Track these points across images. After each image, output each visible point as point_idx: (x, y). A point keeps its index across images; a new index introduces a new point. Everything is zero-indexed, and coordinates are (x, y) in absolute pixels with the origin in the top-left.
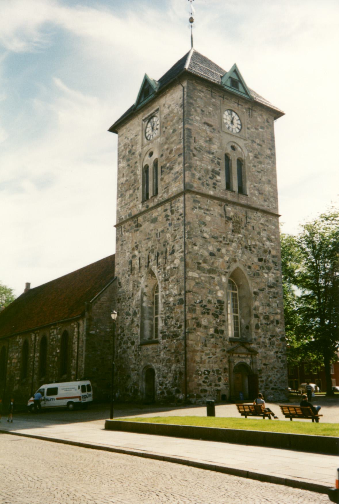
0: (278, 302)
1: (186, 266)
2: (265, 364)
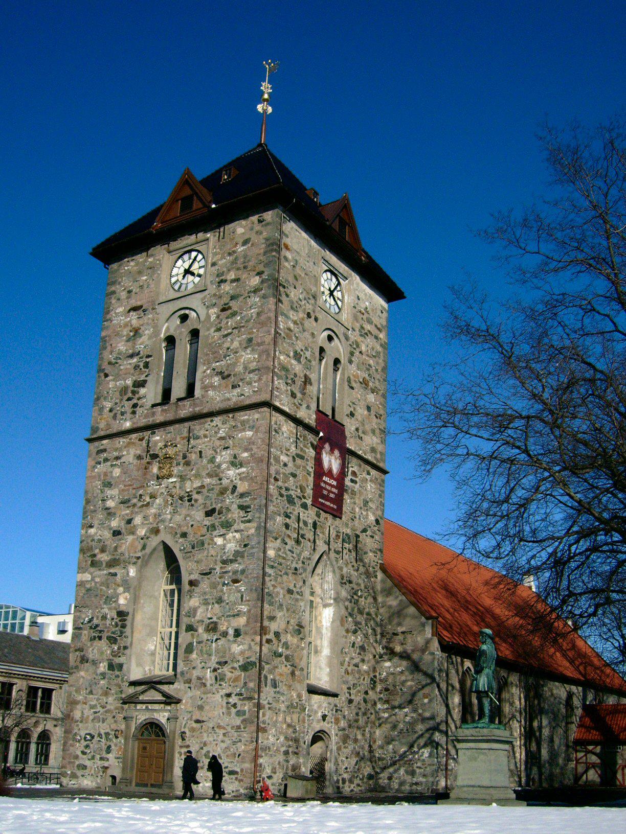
0: (243, 589)
2: (198, 721)
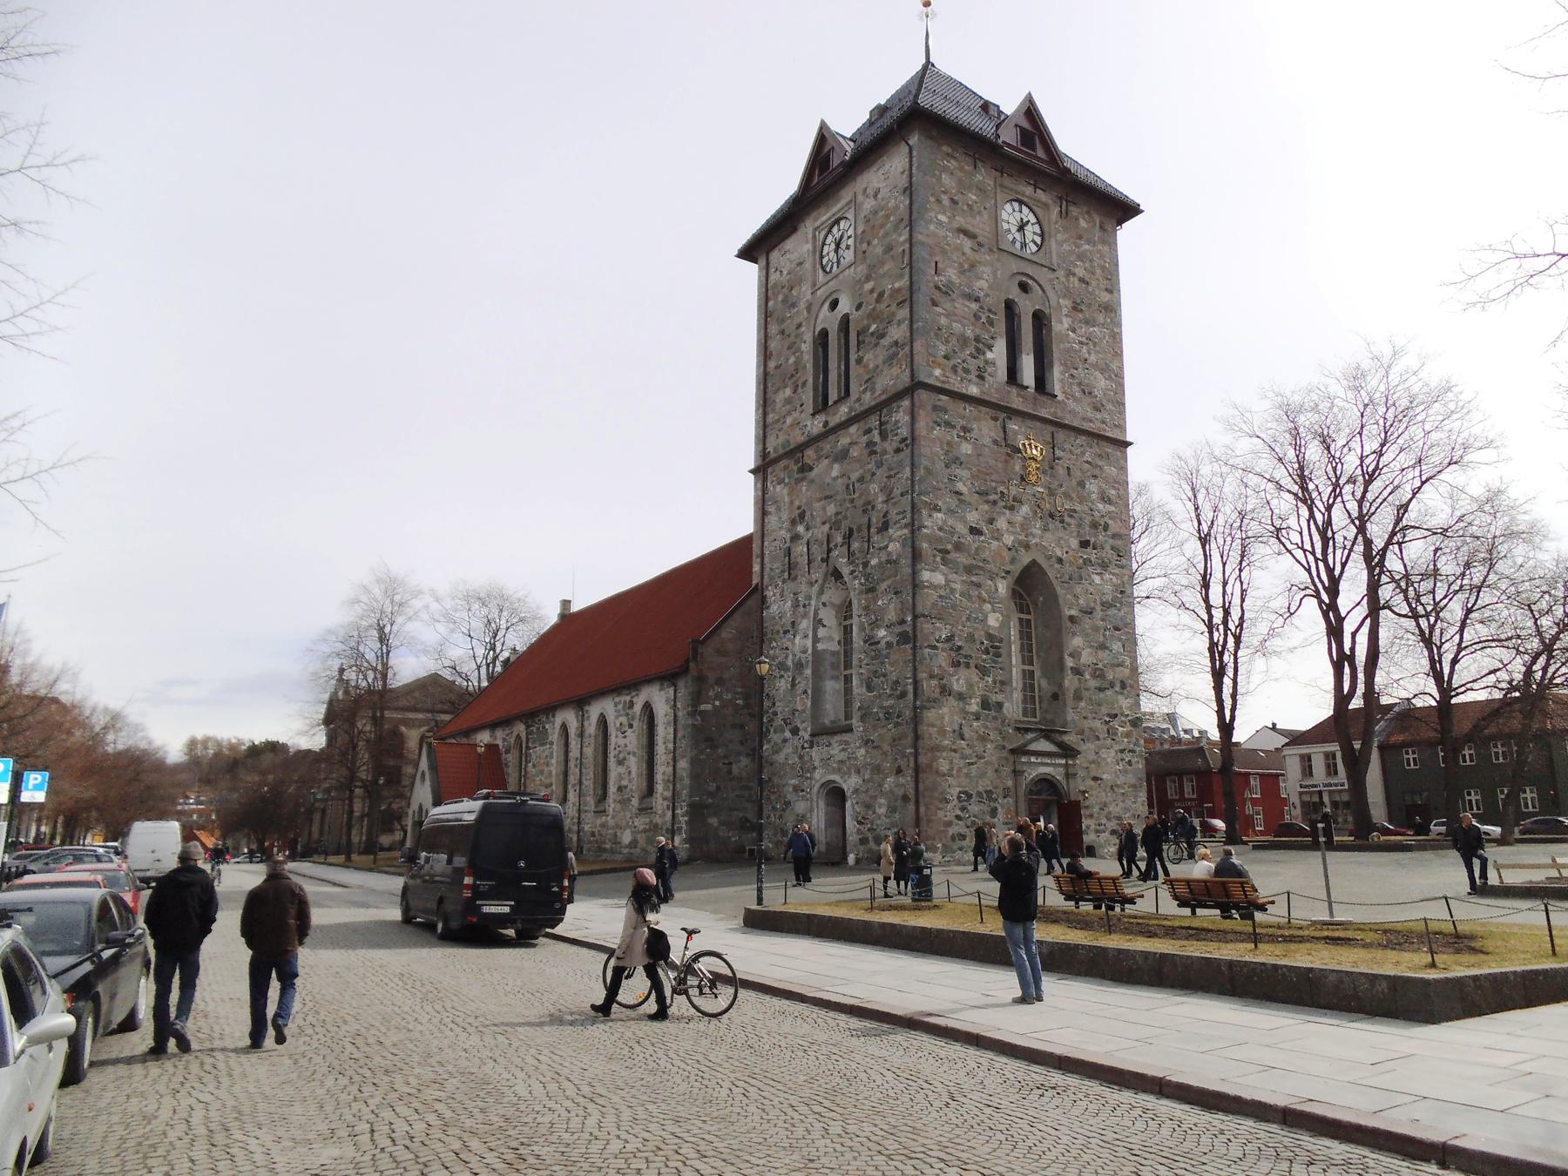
1: (916, 556)
2: (1095, 779)
